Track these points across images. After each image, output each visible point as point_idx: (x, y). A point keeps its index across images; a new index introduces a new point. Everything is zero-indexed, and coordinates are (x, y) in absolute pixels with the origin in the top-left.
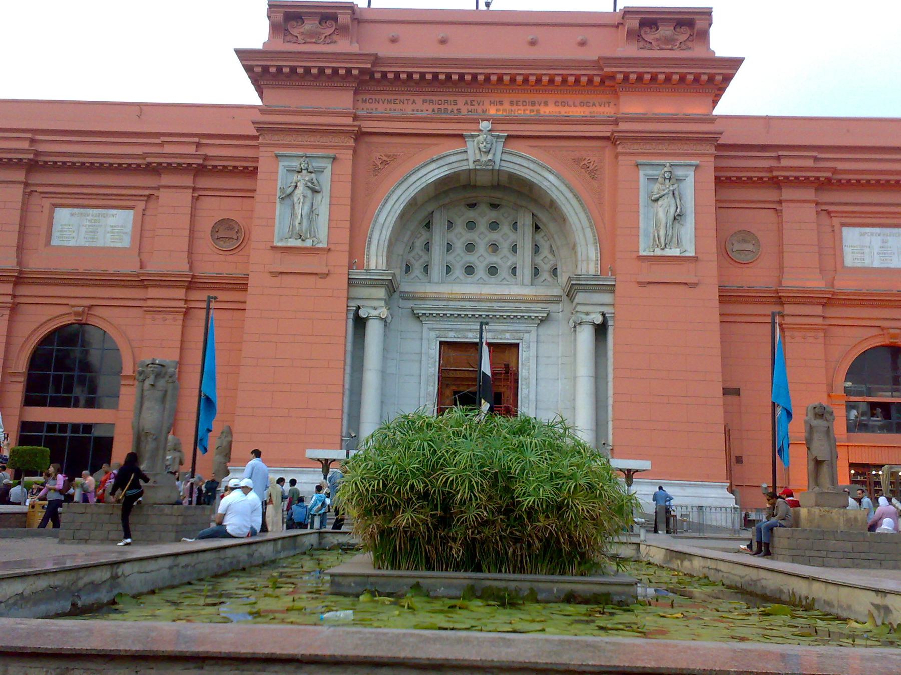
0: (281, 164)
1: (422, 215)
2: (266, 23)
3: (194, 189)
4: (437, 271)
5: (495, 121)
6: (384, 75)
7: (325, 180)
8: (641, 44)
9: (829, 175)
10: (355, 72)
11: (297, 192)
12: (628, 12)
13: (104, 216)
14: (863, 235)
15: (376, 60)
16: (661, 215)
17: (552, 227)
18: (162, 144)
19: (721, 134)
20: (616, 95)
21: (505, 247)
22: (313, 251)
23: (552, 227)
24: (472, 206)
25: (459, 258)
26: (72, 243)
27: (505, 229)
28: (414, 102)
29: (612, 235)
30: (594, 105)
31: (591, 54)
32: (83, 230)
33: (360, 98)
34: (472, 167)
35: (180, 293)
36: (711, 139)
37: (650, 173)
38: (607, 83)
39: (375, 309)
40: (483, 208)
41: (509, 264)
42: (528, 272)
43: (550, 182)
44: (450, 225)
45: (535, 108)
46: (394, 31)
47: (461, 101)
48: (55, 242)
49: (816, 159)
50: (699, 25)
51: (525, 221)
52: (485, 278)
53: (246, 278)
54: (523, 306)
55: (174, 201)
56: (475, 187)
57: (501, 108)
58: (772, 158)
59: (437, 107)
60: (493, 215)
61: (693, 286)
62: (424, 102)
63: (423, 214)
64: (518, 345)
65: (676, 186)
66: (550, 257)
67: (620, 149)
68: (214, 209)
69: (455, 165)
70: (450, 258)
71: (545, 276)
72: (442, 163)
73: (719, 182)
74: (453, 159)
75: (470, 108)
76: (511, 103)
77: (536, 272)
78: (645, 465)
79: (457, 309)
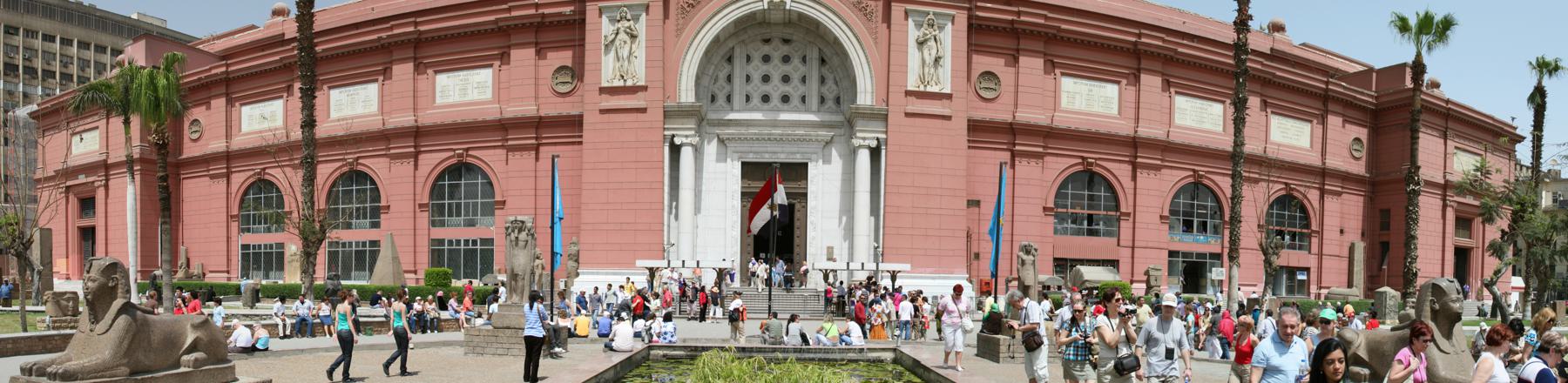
1: (724, 50)
4: (738, 99)
7: (641, 27)
21: (796, 80)
22: (634, 90)
23: (835, 61)
24: (767, 41)
25: (757, 89)
27: (796, 61)
29: (888, 71)
40: (776, 42)
42: (814, 101)
44: (749, 59)
51: (813, 55)
53: (581, 116)
56: (769, 24)
60: (785, 49)
63: (722, 52)
71: (830, 103)
77: (822, 100)
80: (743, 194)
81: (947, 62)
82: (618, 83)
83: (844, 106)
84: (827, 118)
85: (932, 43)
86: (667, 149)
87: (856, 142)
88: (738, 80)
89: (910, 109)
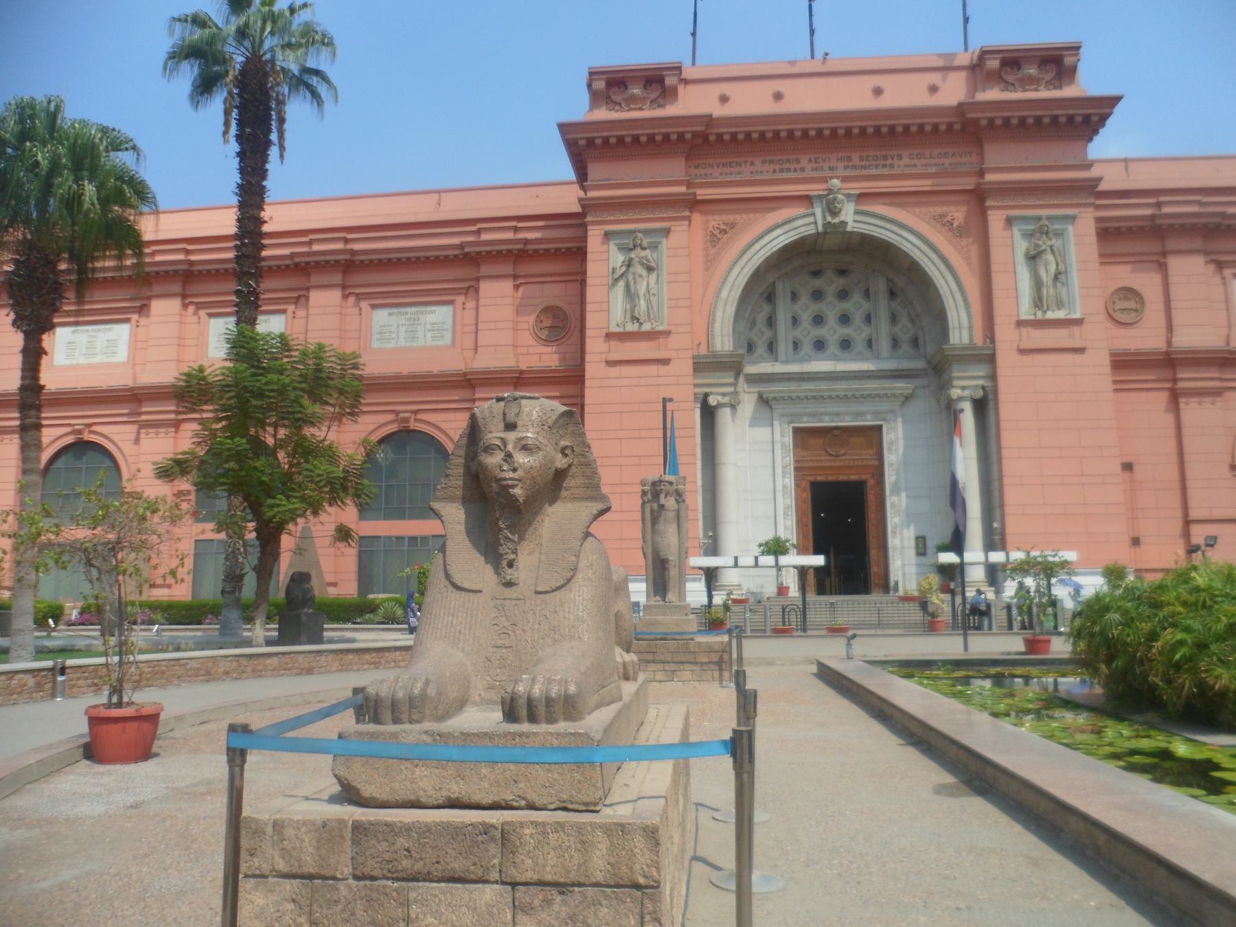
0: (611, 243)
2: (585, 96)
4: (783, 347)
6: (720, 137)
8: (1002, 85)
9: (1217, 220)
11: (631, 270)
12: (984, 54)
13: (421, 313)
15: (708, 120)
18: (479, 232)
19: (1099, 180)
20: (979, 143)
21: (858, 318)
24: (816, 273)
25: (807, 332)
26: (392, 345)
27: (857, 297)
28: (752, 163)
30: (954, 155)
32: (403, 329)
36: (1089, 189)
37: (1024, 227)
39: (724, 395)
41: (863, 335)
42: (884, 345)
44: (794, 297)
45: (890, 161)
46: (726, 88)
47: (804, 160)
48: (375, 344)
49: (1200, 203)
51: (880, 286)
52: (838, 353)
56: (820, 252)
57: (850, 164)
58: (1149, 205)
59: (778, 167)
60: (840, 282)
61: (1080, 350)
62: (764, 162)
64: (880, 428)
65: (1054, 241)
66: (909, 325)
67: (989, 203)
69: (802, 229)
70: (797, 333)
71: (906, 347)
72: (787, 227)
74: (800, 222)
75: (815, 166)
76: (861, 159)
77: (895, 343)
79: (811, 390)
80: (796, 469)
81: (1075, 278)
82: (631, 327)
83: (930, 349)
84: (906, 365)
85: (1050, 257)
86: (698, 412)
87: (955, 393)
89: (1026, 345)
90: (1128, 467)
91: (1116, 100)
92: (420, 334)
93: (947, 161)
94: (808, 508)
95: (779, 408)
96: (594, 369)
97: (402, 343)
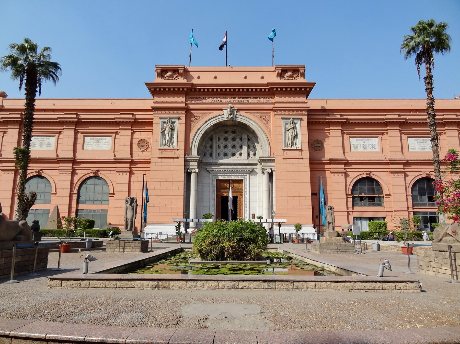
3: (132, 130)
4: (214, 155)
5: (233, 104)
6: (195, 89)
10: (185, 89)
13: (101, 139)
14: (357, 140)
15: (192, 85)
16: (290, 135)
17: (254, 139)
23: (254, 139)
24: (226, 132)
25: (222, 151)
26: (91, 149)
27: (238, 140)
31: (265, 81)
33: (187, 97)
34: (226, 120)
35: (128, 165)
38: (271, 91)
40: (230, 133)
43: (252, 125)
50: (301, 71)
54: (244, 167)
55: (125, 133)
56: (227, 126)
59: (213, 100)
60: (233, 135)
62: (209, 98)
66: (253, 149)
68: (138, 136)
70: (219, 151)
73: (309, 123)
77: (249, 155)
78: (285, 221)
79: (222, 168)
82: (165, 147)
88: (215, 148)
90: (313, 194)
91: (315, 83)
92: (100, 146)
93: (264, 100)
94: (220, 204)
95: (212, 173)
96: (154, 160)
97: (94, 148)
